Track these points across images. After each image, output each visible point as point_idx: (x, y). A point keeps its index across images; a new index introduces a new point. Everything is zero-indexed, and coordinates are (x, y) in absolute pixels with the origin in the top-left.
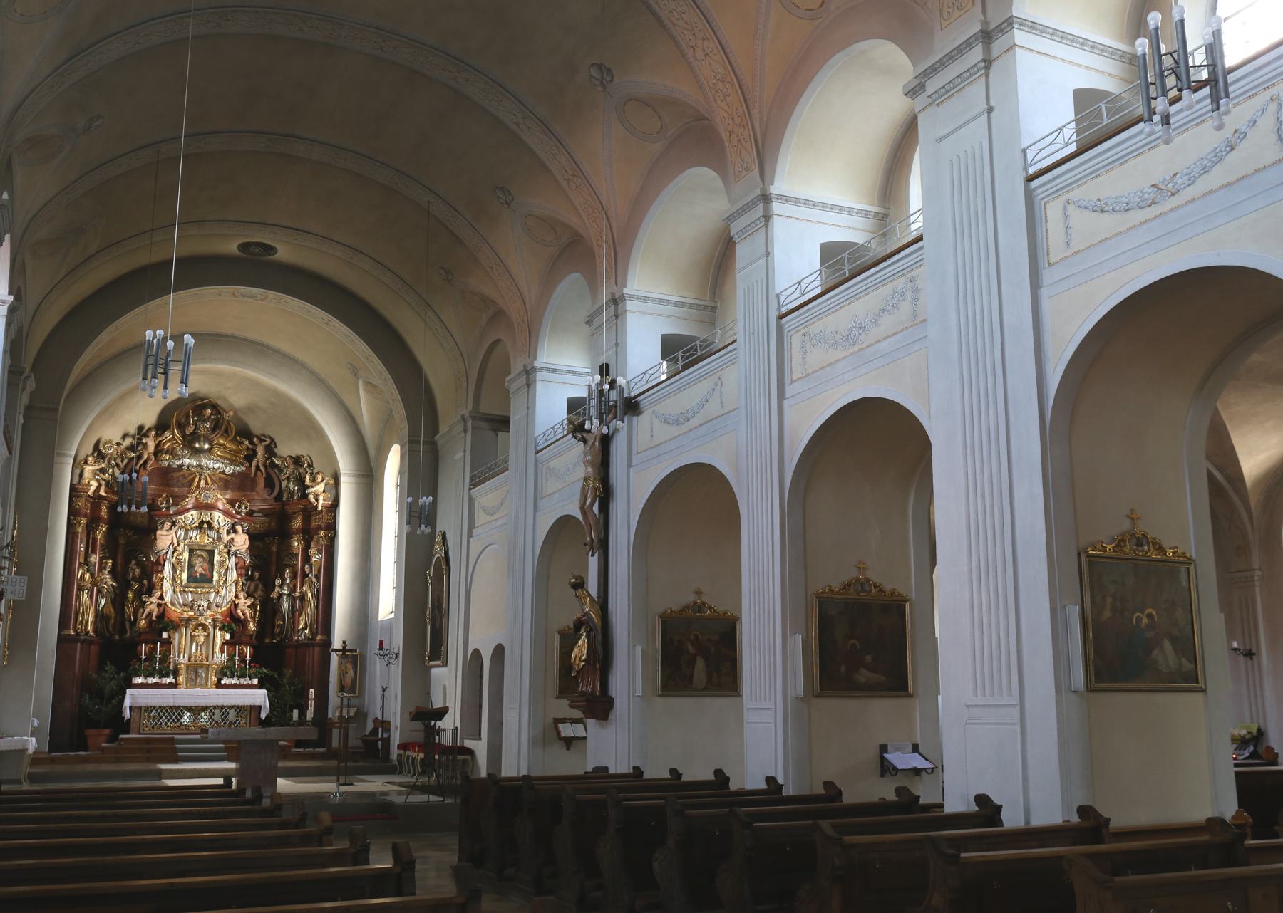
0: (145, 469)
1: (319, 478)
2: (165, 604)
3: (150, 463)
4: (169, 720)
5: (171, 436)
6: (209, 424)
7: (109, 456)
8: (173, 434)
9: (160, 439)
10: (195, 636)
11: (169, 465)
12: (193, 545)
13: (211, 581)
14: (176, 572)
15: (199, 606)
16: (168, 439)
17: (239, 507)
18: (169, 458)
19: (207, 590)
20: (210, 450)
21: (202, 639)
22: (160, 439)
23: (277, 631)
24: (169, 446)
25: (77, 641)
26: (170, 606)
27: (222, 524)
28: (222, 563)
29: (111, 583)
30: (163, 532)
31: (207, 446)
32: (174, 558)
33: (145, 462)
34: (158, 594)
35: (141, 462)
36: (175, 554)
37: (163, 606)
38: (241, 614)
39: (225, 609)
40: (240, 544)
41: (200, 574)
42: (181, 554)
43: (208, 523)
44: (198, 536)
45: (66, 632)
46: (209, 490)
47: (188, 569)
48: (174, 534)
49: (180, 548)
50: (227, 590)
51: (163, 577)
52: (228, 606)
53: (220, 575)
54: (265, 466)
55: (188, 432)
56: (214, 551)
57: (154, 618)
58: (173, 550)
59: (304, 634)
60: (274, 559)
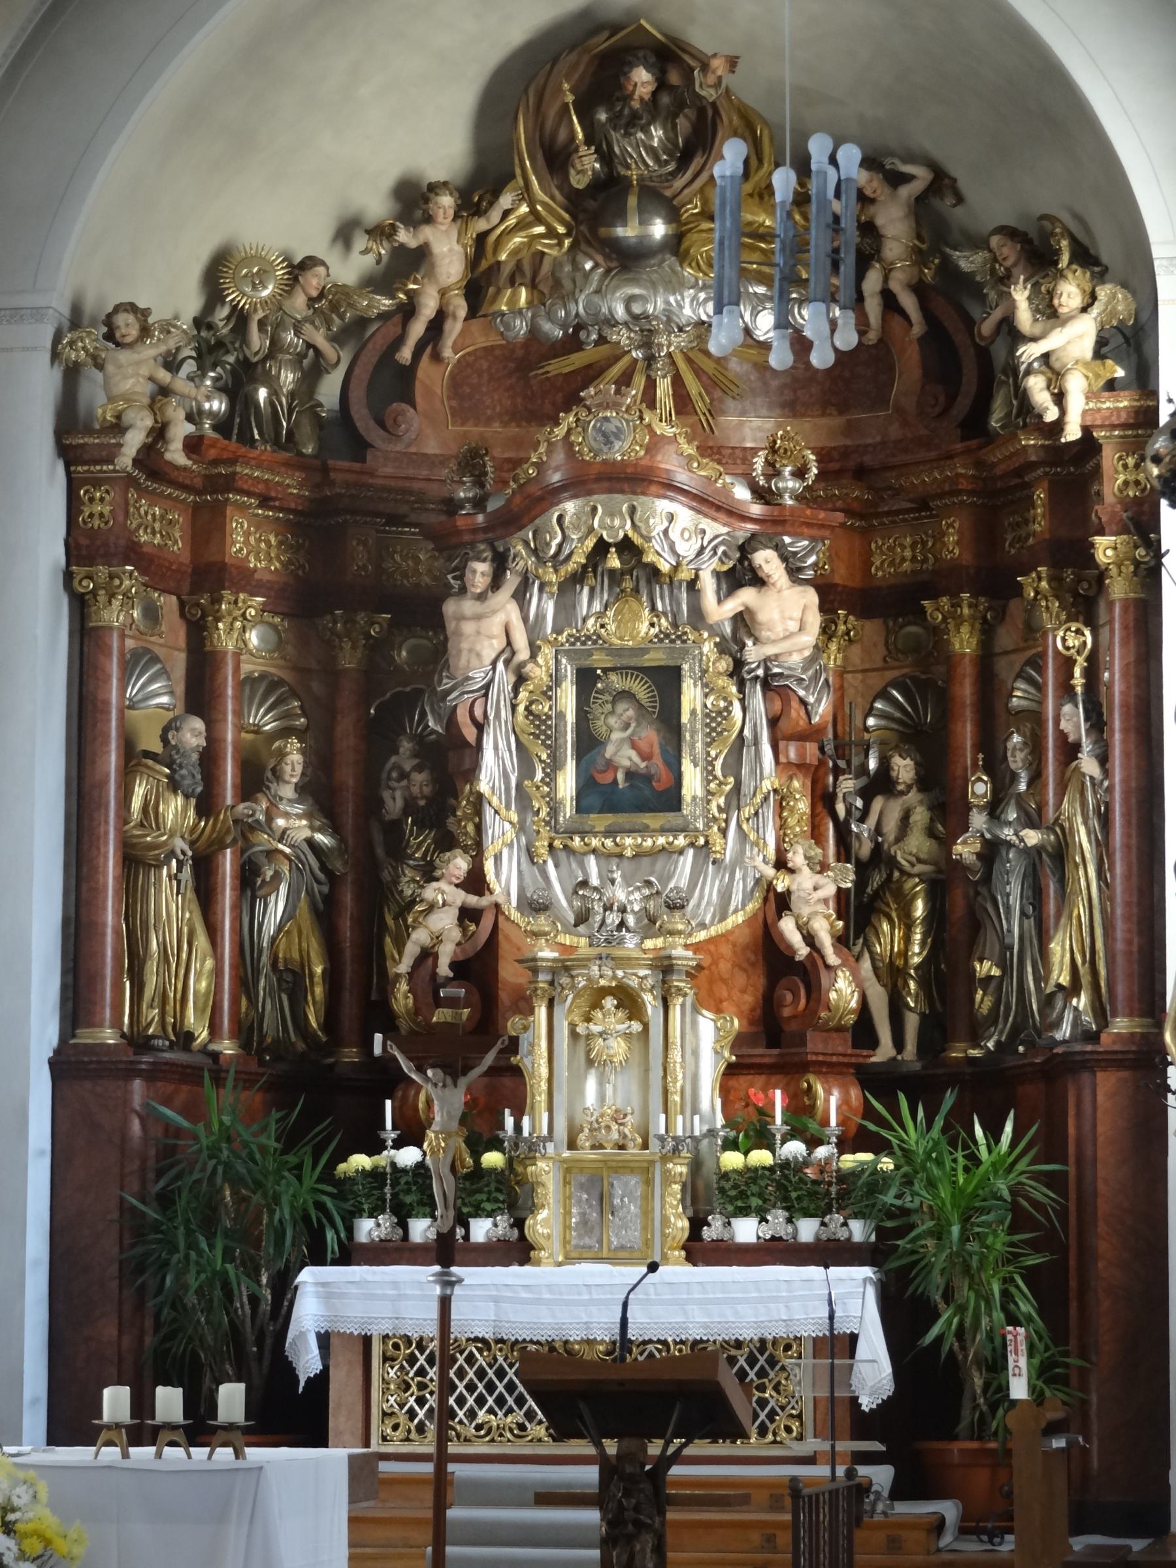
0: (437, 357)
1: (1070, 294)
2: (497, 906)
3: (454, 329)
4: (481, 1401)
5: (524, 209)
6: (657, 134)
7: (260, 314)
8: (526, 194)
9: (481, 225)
10: (589, 1036)
11: (533, 331)
12: (589, 653)
13: (671, 800)
14: (532, 776)
15: (608, 908)
16: (512, 221)
17: (773, 472)
18: (530, 303)
19: (661, 841)
20: (676, 245)
21: (618, 1048)
22: (481, 225)
23: (983, 1001)
24: (516, 252)
25: (131, 1072)
26: (515, 915)
27: (687, 549)
28: (716, 719)
29: (307, 833)
30: (468, 606)
31: (659, 229)
32: (521, 708)
33: (436, 326)
34: (460, 864)
35: (418, 329)
36: (523, 695)
37: (487, 922)
38: (795, 938)
39: (740, 918)
40: (779, 631)
41: (630, 775)
42: (548, 693)
43: (627, 547)
44: (610, 613)
45: (85, 1037)
46: (615, 406)
47: (579, 756)
48: (512, 612)
49: (539, 673)
50: (742, 835)
51: (480, 796)
52: (753, 906)
53: (708, 774)
54: (919, 289)
55: (579, 181)
56: (678, 669)
57: (444, 969)
58: (512, 679)
59: (1068, 1017)
60: (966, 691)
